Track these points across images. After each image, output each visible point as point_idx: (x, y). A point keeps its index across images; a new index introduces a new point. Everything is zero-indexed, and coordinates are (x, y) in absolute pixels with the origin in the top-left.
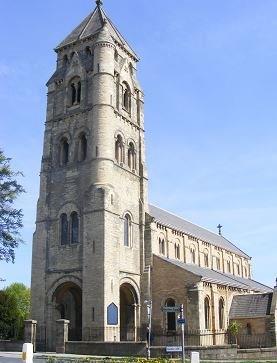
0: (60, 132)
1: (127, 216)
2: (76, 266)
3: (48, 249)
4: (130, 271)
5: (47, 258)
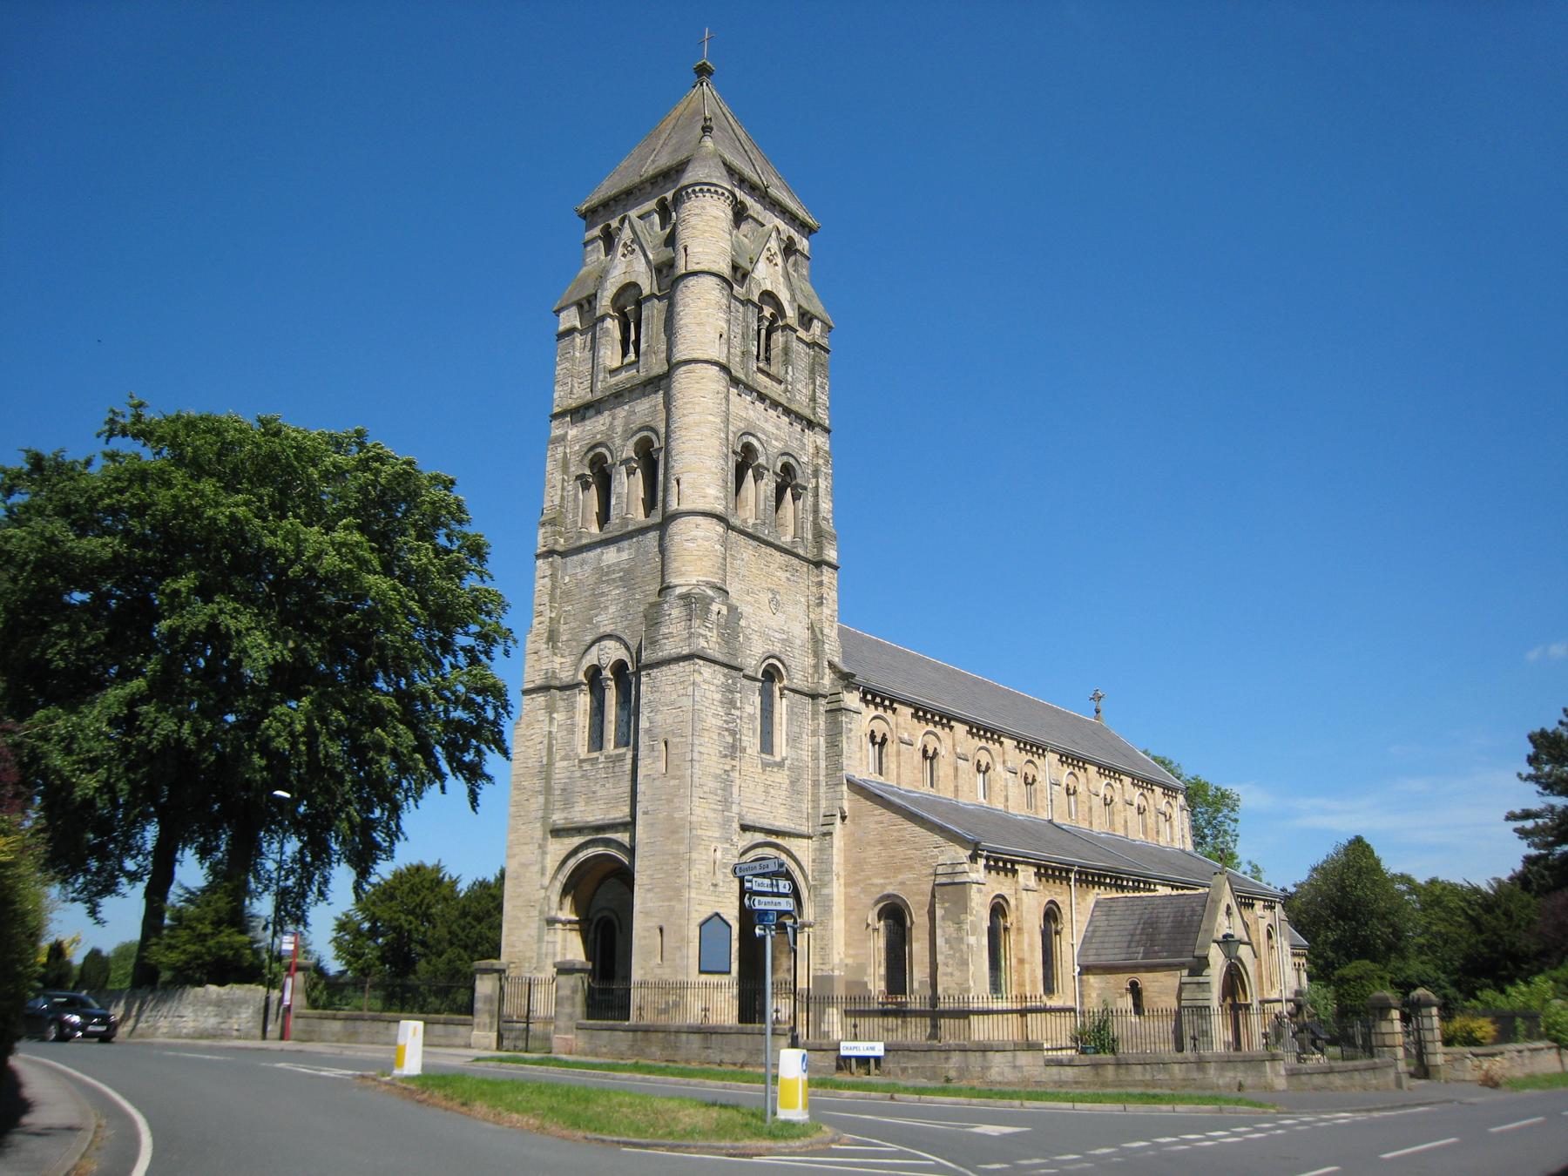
0: (587, 441)
1: (771, 675)
2: (621, 813)
3: (550, 764)
4: (780, 824)
5: (548, 790)
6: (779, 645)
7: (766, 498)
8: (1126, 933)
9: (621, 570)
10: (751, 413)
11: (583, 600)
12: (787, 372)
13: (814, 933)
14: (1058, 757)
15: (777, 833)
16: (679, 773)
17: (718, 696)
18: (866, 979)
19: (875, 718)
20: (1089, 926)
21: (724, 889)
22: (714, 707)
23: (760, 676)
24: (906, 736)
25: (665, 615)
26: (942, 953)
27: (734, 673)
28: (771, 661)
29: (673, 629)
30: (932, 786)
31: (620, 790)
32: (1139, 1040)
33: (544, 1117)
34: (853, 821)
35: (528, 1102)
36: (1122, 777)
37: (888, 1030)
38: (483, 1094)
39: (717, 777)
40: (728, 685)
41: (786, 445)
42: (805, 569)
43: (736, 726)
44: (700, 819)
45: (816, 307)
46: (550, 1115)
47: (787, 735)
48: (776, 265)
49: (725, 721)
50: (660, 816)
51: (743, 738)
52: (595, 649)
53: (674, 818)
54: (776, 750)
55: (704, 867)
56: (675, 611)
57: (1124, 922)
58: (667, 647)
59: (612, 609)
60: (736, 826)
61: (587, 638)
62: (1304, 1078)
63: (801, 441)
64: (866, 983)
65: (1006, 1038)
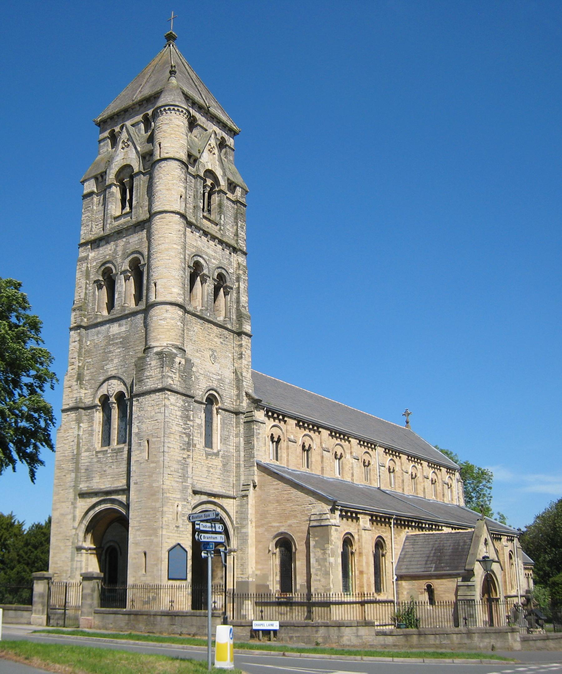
1: (211, 400)
2: (121, 483)
4: (217, 490)
6: (216, 382)
7: (208, 294)
8: (424, 555)
9: (121, 337)
10: (199, 243)
11: (98, 355)
12: (220, 218)
13: (237, 556)
14: (384, 450)
15: (215, 496)
16: (156, 459)
17: (179, 413)
18: (268, 583)
19: (274, 426)
20: (402, 551)
21: (183, 529)
22: (177, 420)
23: (204, 401)
24: (292, 437)
25: (147, 364)
26: (314, 568)
27: (189, 399)
28: (211, 392)
29: (152, 373)
30: (308, 467)
31: (120, 470)
32: (432, 620)
33: (75, 666)
34: (260, 488)
35: (65, 657)
36: (422, 462)
37: (281, 614)
38: (38, 652)
39: (178, 461)
40: (185, 406)
41: (220, 263)
42: (232, 337)
43: (190, 431)
44: (168, 487)
45: (238, 179)
46: (79, 665)
47: (221, 436)
48: (214, 154)
49: (184, 429)
50: (145, 485)
51: (194, 438)
52: (105, 385)
53: (153, 487)
54: (214, 445)
55: (171, 516)
56: (154, 362)
57: (423, 549)
58: (149, 384)
59: (116, 361)
60: (190, 491)
61: (101, 378)
62: (531, 643)
63: (229, 260)
64: (268, 586)
65: (352, 619)
